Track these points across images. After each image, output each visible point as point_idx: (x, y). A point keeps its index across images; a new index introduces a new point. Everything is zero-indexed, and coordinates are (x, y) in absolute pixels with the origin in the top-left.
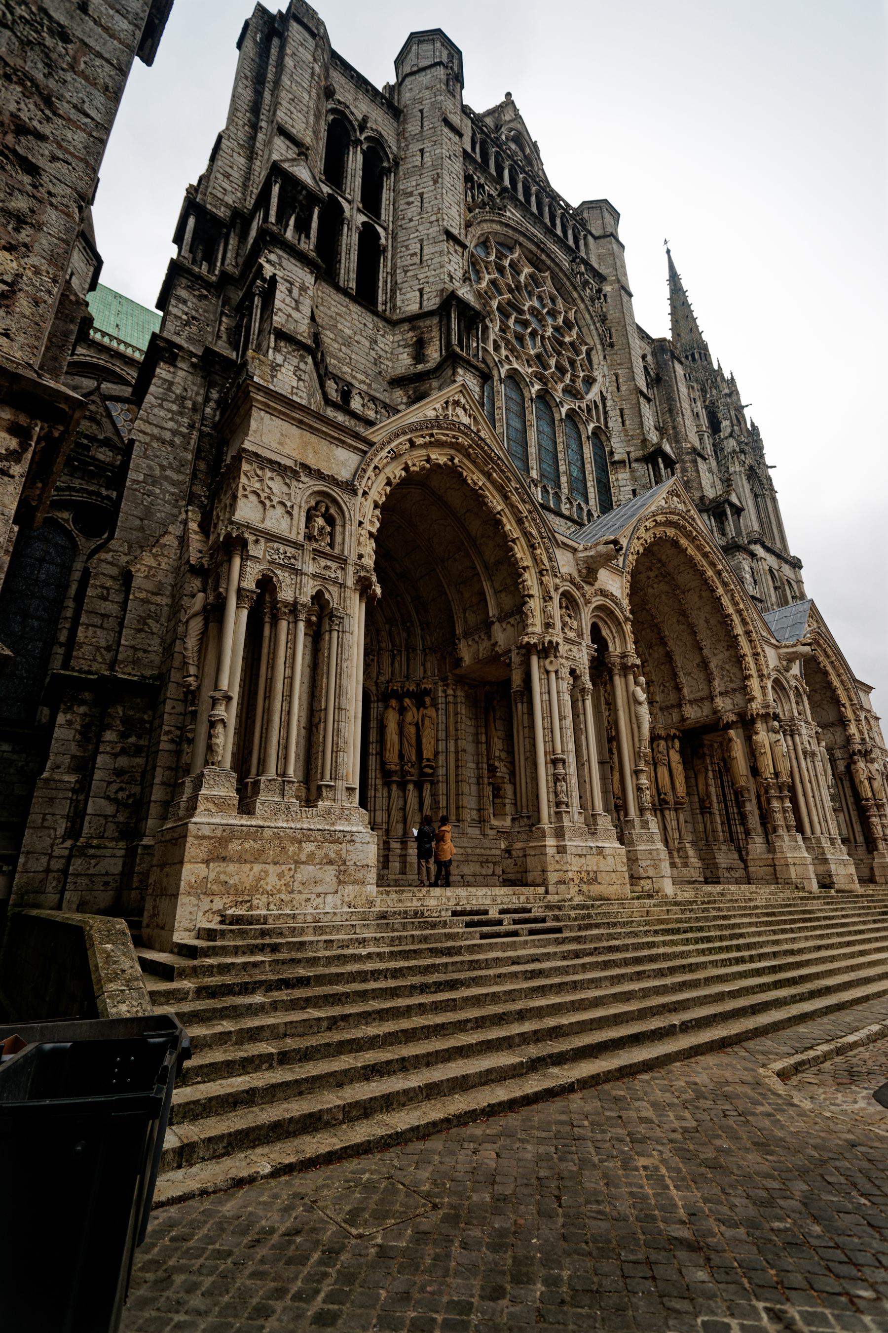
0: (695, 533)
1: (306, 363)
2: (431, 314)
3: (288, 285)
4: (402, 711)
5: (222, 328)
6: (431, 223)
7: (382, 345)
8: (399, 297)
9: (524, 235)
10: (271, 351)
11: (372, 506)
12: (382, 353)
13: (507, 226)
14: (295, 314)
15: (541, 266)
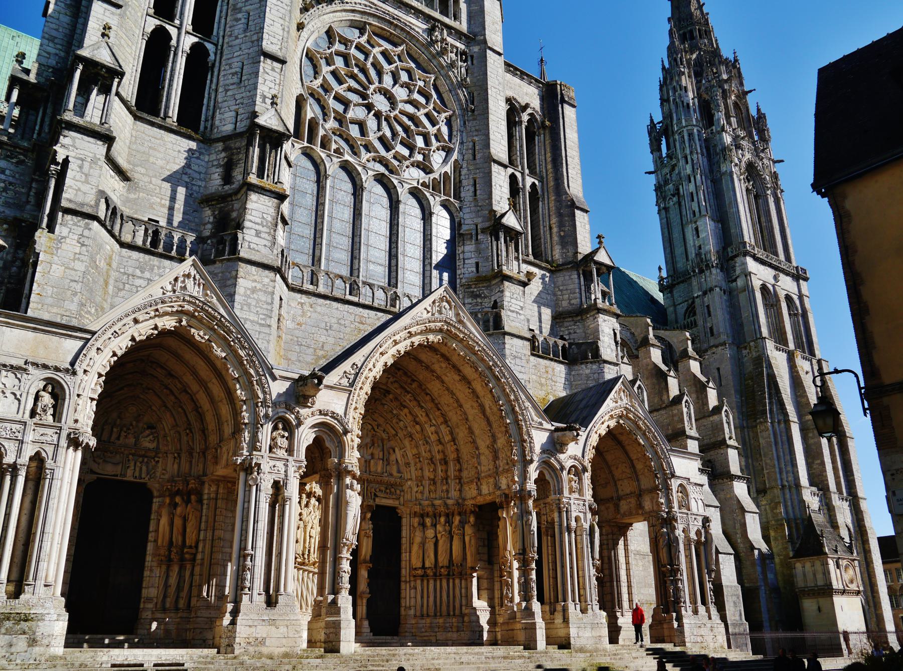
0: (462, 336)
1: (90, 229)
2: (241, 135)
3: (80, 162)
4: (175, 505)
5: (32, 193)
6: (252, 42)
7: (195, 167)
8: (218, 116)
9: (374, 16)
10: (58, 226)
11: (97, 376)
12: (196, 176)
13: (353, 11)
14: (85, 188)
15: (396, 40)
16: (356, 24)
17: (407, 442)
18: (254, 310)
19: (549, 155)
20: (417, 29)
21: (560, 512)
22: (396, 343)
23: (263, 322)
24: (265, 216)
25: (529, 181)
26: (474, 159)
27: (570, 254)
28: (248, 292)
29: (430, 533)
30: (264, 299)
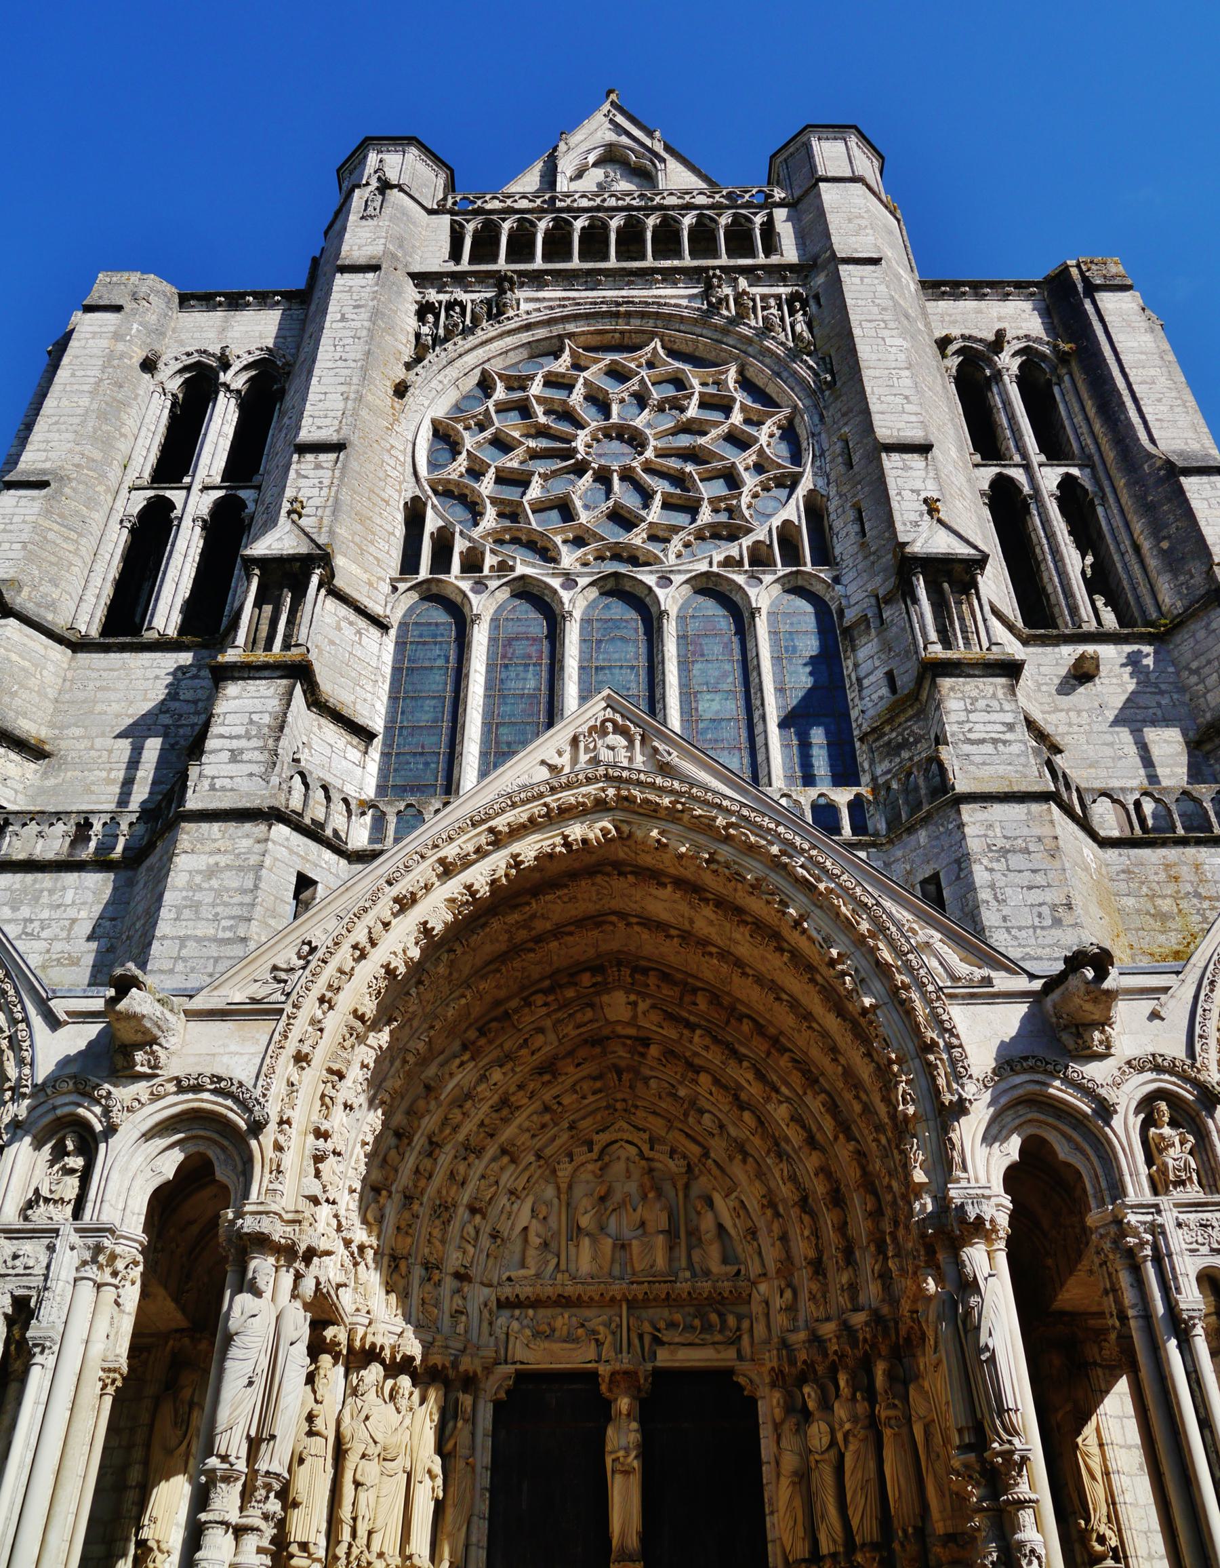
0: (666, 801)
9: (575, 317)
12: (187, 708)
13: (528, 327)
15: (637, 339)
16: (545, 346)
17: (738, 1171)
18: (206, 912)
19: (1089, 404)
20: (673, 301)
21: (1136, 1270)
22: (447, 870)
23: (228, 935)
24: (255, 717)
25: (1050, 478)
26: (850, 465)
27: (1198, 580)
28: (198, 879)
29: (818, 1434)
30: (235, 884)
